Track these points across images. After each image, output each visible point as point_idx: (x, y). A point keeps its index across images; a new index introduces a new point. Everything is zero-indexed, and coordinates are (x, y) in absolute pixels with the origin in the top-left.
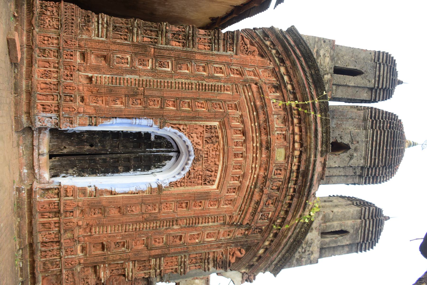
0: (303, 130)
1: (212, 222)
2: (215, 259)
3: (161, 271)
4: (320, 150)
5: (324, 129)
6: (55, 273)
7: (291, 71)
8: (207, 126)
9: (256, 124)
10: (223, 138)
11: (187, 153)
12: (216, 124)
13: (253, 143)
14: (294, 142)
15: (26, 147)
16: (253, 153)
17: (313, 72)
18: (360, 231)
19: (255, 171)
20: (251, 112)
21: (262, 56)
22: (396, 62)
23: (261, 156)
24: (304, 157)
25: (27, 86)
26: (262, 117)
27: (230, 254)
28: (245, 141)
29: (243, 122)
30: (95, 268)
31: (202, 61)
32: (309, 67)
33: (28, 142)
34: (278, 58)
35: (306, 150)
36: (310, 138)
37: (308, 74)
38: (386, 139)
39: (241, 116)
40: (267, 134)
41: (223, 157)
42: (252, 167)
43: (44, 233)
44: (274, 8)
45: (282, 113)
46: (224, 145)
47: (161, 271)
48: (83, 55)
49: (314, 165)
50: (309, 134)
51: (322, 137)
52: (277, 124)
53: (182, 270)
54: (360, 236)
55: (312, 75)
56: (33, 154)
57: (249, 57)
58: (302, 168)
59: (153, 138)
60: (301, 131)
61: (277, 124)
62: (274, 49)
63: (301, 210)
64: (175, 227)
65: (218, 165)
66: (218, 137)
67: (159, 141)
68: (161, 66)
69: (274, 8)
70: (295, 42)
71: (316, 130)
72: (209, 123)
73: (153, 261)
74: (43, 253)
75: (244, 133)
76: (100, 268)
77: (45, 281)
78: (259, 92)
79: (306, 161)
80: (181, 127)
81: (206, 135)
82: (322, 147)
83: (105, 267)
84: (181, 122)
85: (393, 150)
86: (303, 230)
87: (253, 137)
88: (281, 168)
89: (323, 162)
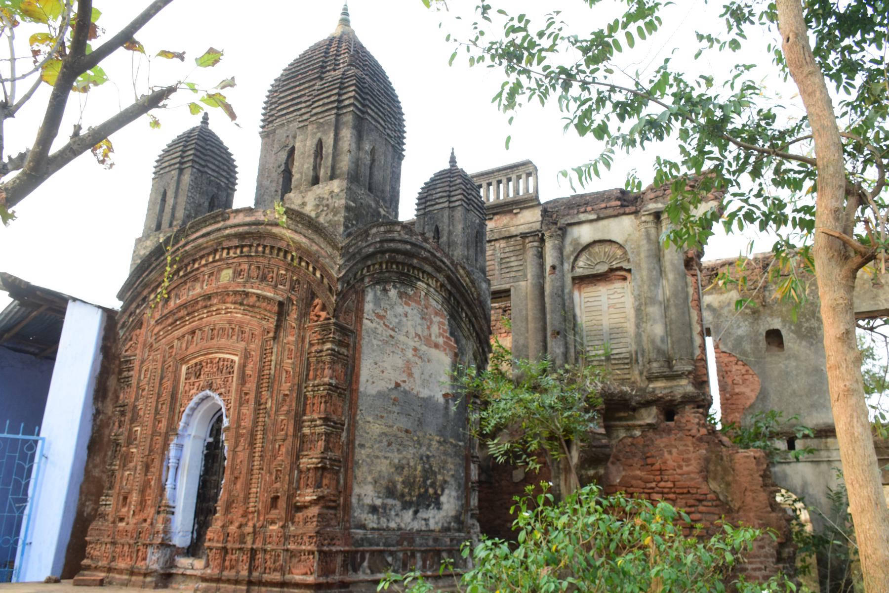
0: (202, 253)
3: (320, 418)
4: (222, 223)
5: (203, 225)
6: (288, 558)
7: (153, 286)
8: (186, 379)
10: (195, 358)
12: (184, 368)
13: (203, 318)
14: (214, 261)
15: (183, 582)
17: (153, 259)
18: (321, 121)
21: (142, 324)
24: (225, 245)
25: (127, 574)
26: (183, 313)
28: (200, 329)
29: (183, 336)
30: (299, 508)
31: (137, 392)
32: (150, 265)
33: (180, 579)
35: (220, 243)
36: (207, 242)
37: (157, 263)
39: (178, 339)
40: (197, 302)
43: (240, 568)
45: (188, 284)
47: (320, 418)
48: (121, 520)
51: (210, 224)
52: (198, 290)
55: (156, 260)
56: (191, 576)
57: (141, 340)
58: (236, 242)
59: (211, 440)
60: (202, 257)
61: (198, 290)
62: (135, 312)
63: (275, 230)
64: (269, 405)
66: (196, 364)
67: (214, 432)
68: (135, 439)
71: (203, 236)
73: (306, 431)
74: (267, 571)
75: (193, 333)
76: (298, 502)
77: (294, 571)
78: (161, 323)
79: (230, 240)
80: (182, 409)
81: (193, 379)
83: (299, 495)
85: (301, 74)
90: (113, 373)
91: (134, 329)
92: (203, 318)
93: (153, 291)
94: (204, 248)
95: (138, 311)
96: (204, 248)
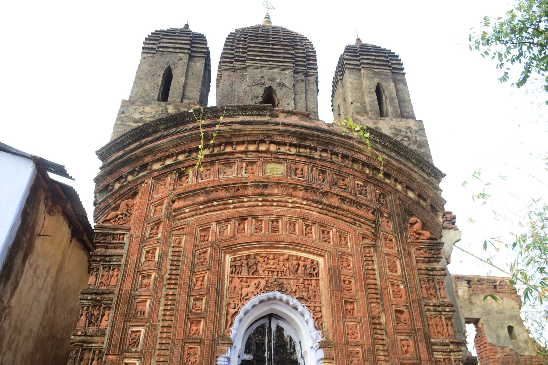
0: (242, 139)
1: (373, 264)
2: (427, 259)
3: (452, 343)
4: (269, 118)
7: (159, 155)
8: (232, 272)
9: (231, 201)
10: (249, 249)
11: (271, 302)
12: (228, 258)
13: (258, 206)
14: (258, 151)
16: (272, 206)
17: (162, 127)
18: (376, 70)
19: (297, 203)
20: (213, 208)
21: (136, 194)
22: (159, 30)
23: (277, 195)
24: (278, 138)
26: (221, 194)
27: (418, 238)
28: (254, 217)
29: (227, 220)
31: (135, 280)
32: (156, 132)
34: (139, 172)
35: (269, 136)
36: (252, 130)
37: (165, 133)
38: (259, 45)
39: (218, 222)
41: (278, 248)
42: (292, 207)
44: (74, 179)
45: (217, 167)
46: (260, 248)
47: (452, 343)
49: (290, 125)
50: (247, 132)
51: (252, 115)
52: (232, 174)
53: (447, 310)
54: (383, 70)
55: (166, 129)
57: (135, 211)
58: (293, 140)
59: (249, 357)
60: (243, 143)
61: (232, 174)
62: (126, 177)
63: (351, 142)
64: (383, 320)
65: (289, 256)
66: (248, 256)
67: (253, 347)
68: (136, 343)
69: (74, 179)
70: (119, 150)
71: (242, 123)
72: (228, 269)
73: (438, 356)
75: (243, 219)
78: (185, 198)
79: (284, 136)
80: (232, 311)
81: (244, 274)
82: (265, 116)
84: (224, 312)
86: (378, 140)
87: (249, 206)
88: (294, 168)
89: (286, 115)
90: (22, 250)
91: (122, 197)
92: (258, 206)
93: (159, 160)
94: (245, 135)
95: (130, 178)
96: (245, 135)
